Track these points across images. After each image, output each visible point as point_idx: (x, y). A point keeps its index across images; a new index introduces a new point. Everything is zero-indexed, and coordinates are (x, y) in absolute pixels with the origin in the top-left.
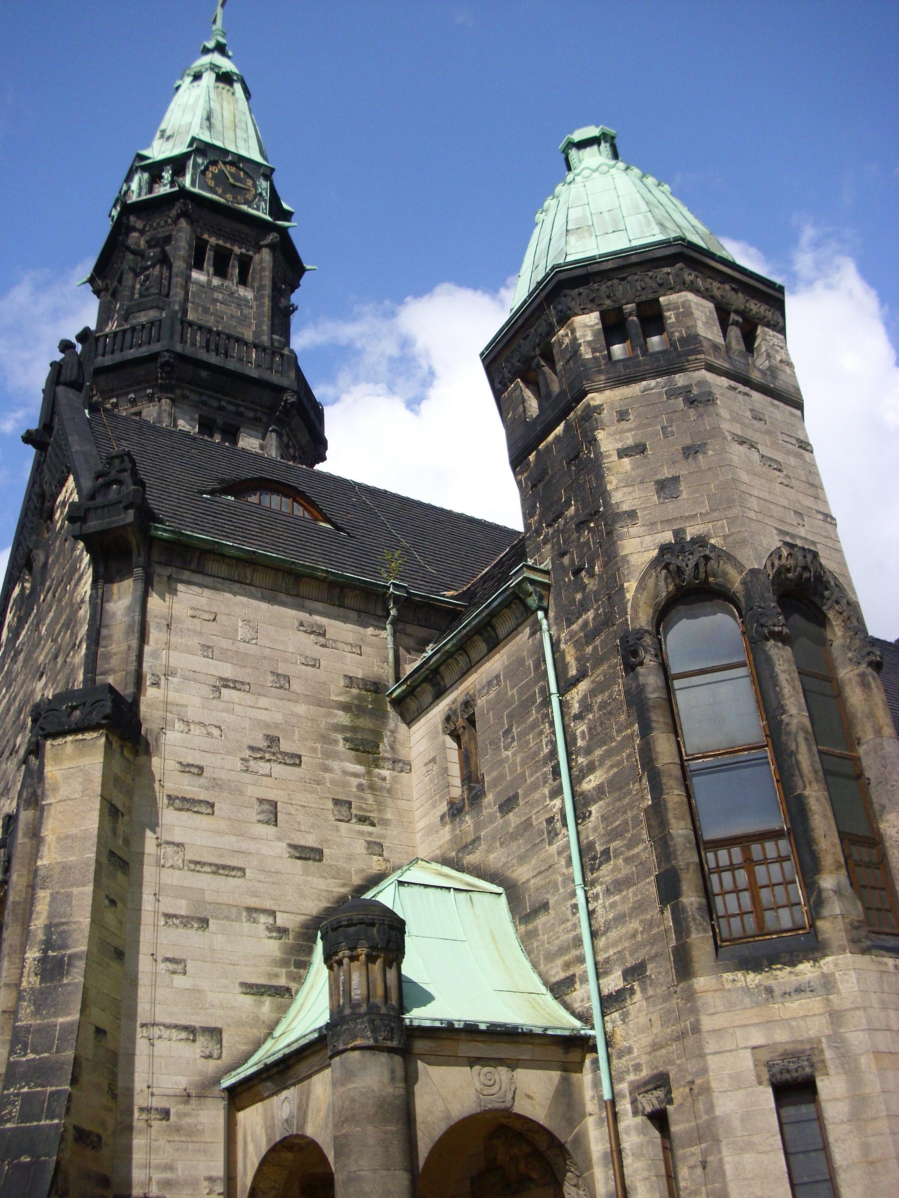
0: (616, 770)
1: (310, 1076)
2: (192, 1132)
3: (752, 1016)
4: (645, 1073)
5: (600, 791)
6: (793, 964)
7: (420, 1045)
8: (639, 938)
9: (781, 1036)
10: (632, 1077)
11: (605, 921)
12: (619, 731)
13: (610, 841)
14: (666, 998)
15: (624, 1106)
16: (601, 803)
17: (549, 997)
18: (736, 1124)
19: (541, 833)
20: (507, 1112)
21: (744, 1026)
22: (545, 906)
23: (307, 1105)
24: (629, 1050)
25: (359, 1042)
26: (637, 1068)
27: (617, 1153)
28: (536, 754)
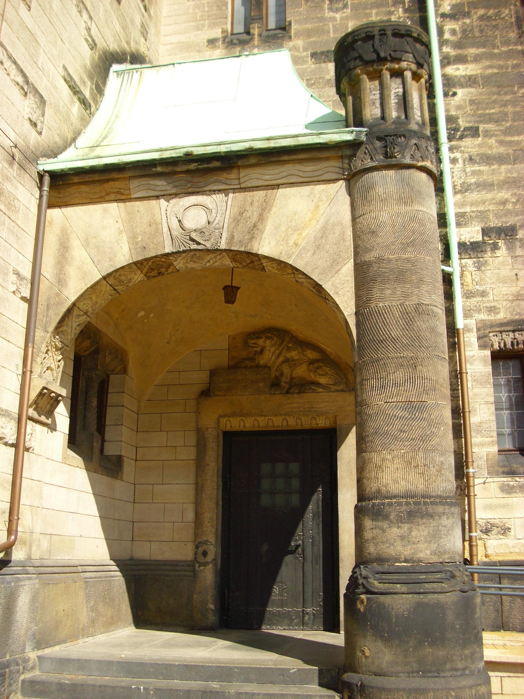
0: (495, 71)
1: (278, 186)
4: (502, 316)
8: (510, 206)
10: (483, 316)
11: (464, 183)
13: (481, 122)
16: (472, 90)
23: (261, 218)
24: (483, 294)
26: (492, 310)
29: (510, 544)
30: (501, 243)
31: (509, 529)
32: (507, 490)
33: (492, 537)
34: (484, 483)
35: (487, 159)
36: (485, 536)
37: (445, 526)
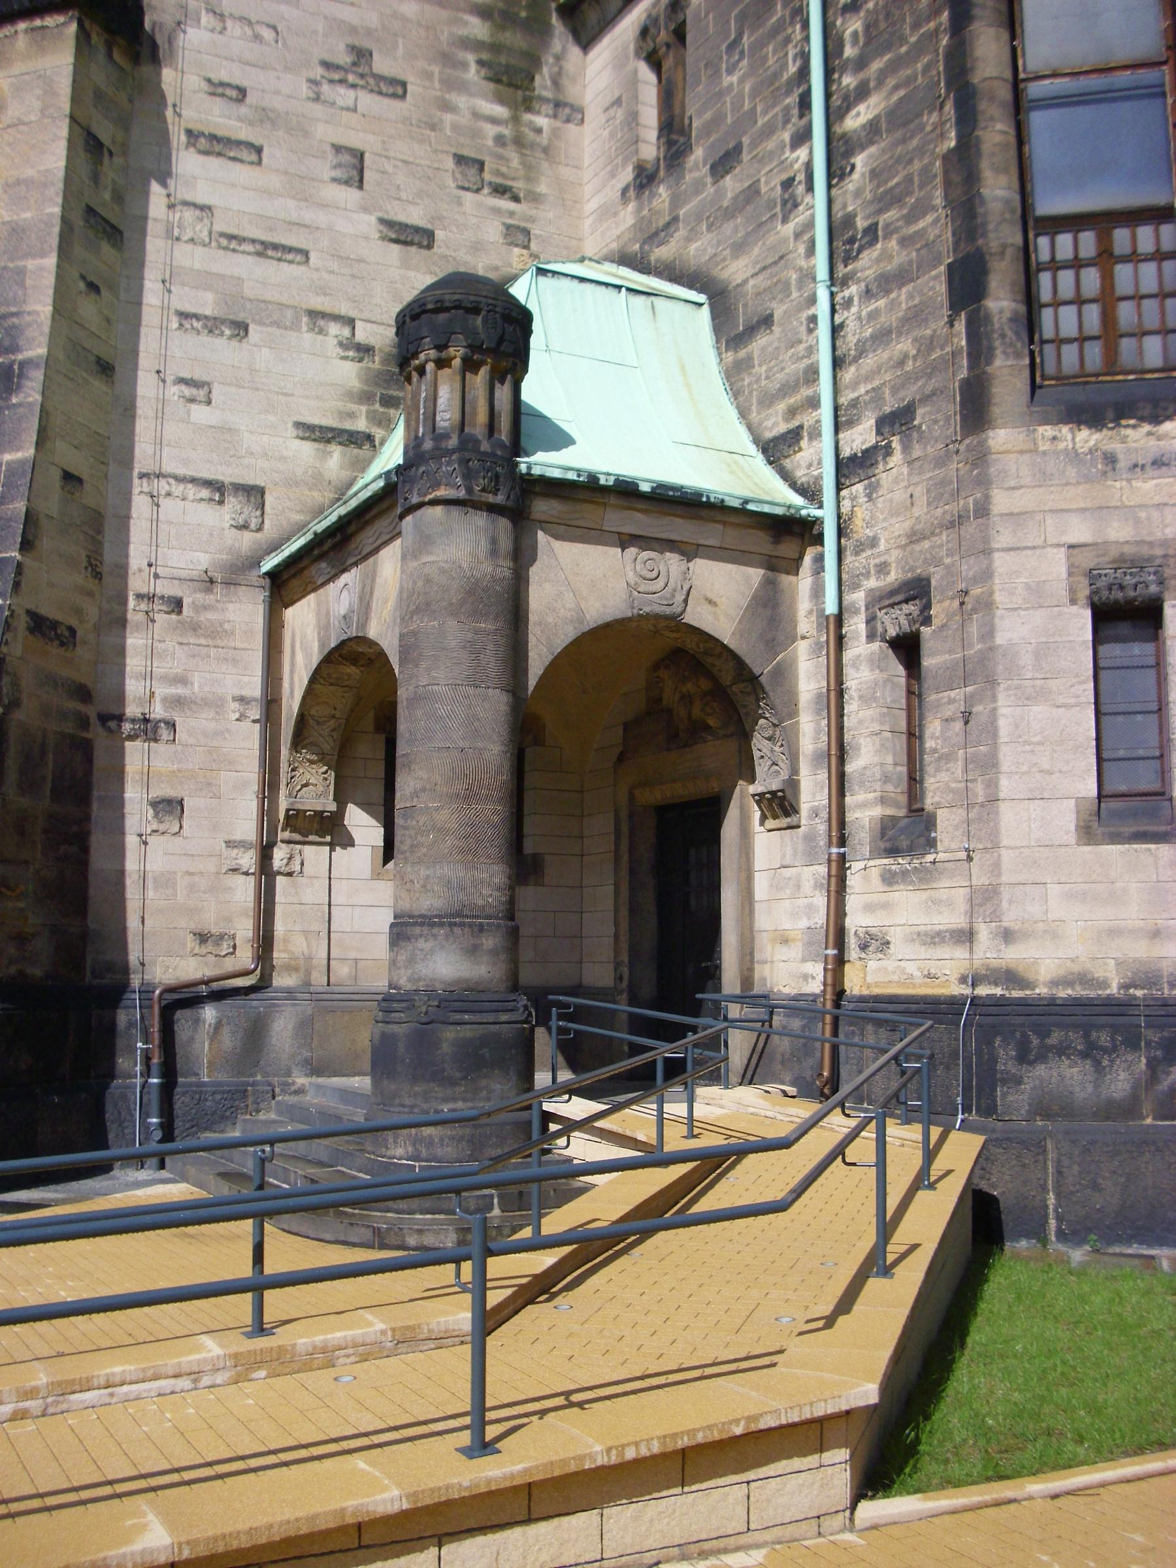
0: (902, 93)
1: (376, 550)
2: (216, 633)
3: (1075, 496)
4: (894, 576)
5: (873, 129)
6: (1156, 420)
7: (542, 507)
8: (909, 366)
9: (1119, 532)
10: (872, 583)
11: (859, 341)
12: (916, 26)
13: (880, 211)
14: (940, 462)
15: (856, 626)
16: (873, 149)
17: (759, 460)
18: (1026, 659)
19: (771, 204)
20: (674, 623)
21: (1062, 510)
22: (767, 321)
23: (371, 594)
24: (873, 542)
25: (442, 492)
26: (883, 568)
27: (837, 692)
28: (776, 76)
29: (890, 969)
30: (896, 443)
31: (888, 943)
32: (889, 879)
33: (871, 956)
34: (865, 869)
35: (901, 277)
36: (863, 955)
37: (422, 950)
